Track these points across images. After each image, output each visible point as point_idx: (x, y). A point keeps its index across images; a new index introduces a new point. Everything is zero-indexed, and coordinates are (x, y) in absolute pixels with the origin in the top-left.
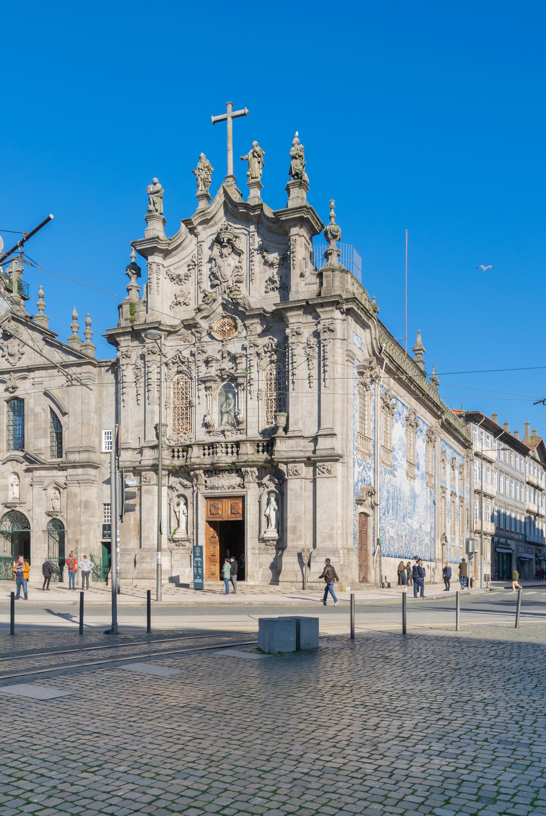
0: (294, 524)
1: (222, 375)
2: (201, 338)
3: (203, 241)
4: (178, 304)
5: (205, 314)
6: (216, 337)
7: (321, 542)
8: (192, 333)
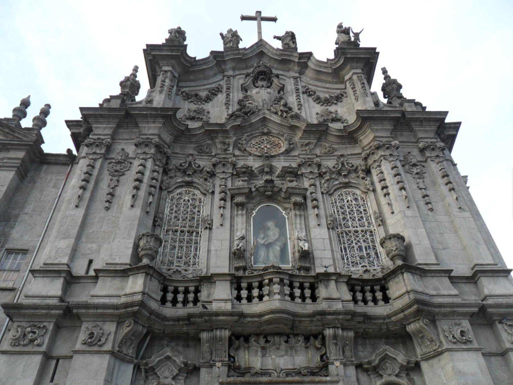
2: (226, 150)
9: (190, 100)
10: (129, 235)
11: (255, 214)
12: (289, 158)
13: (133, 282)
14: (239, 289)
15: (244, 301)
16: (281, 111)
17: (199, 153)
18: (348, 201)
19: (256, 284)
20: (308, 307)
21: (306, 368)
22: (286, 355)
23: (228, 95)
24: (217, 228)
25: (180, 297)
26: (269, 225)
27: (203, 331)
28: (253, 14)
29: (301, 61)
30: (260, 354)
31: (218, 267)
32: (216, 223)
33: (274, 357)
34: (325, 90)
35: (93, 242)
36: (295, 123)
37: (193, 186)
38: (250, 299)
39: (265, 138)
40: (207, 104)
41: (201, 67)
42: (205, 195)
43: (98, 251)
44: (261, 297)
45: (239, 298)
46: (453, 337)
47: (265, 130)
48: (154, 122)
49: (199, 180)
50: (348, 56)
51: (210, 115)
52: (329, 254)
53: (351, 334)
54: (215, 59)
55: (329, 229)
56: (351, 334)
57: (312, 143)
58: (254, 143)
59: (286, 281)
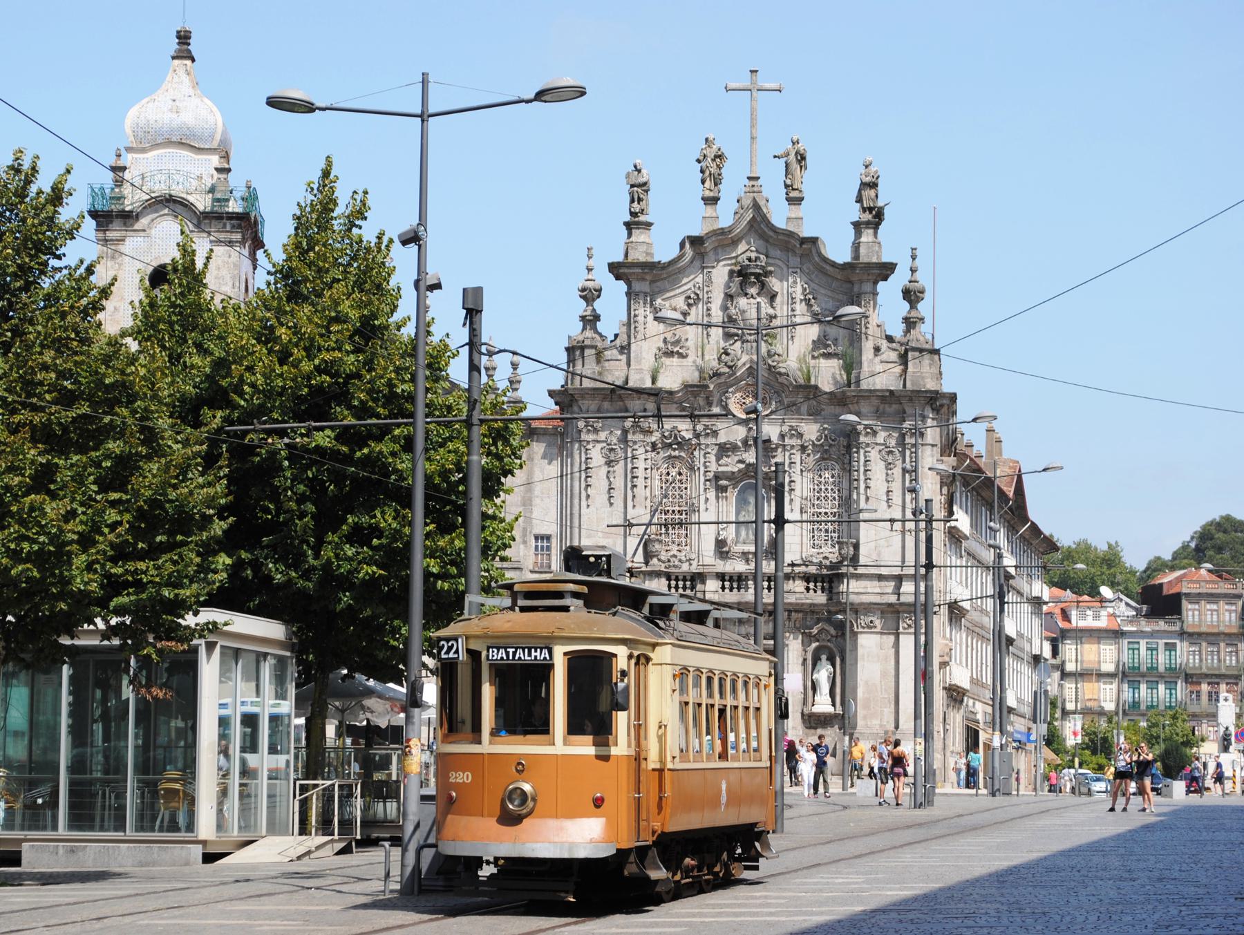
4: (670, 354)
14: (723, 580)
15: (727, 591)
23: (708, 310)
25: (681, 584)
28: (746, 83)
32: (702, 507)
34: (829, 293)
38: (731, 589)
44: (739, 589)
45: (723, 588)
51: (689, 344)
52: (798, 539)
53: (800, 615)
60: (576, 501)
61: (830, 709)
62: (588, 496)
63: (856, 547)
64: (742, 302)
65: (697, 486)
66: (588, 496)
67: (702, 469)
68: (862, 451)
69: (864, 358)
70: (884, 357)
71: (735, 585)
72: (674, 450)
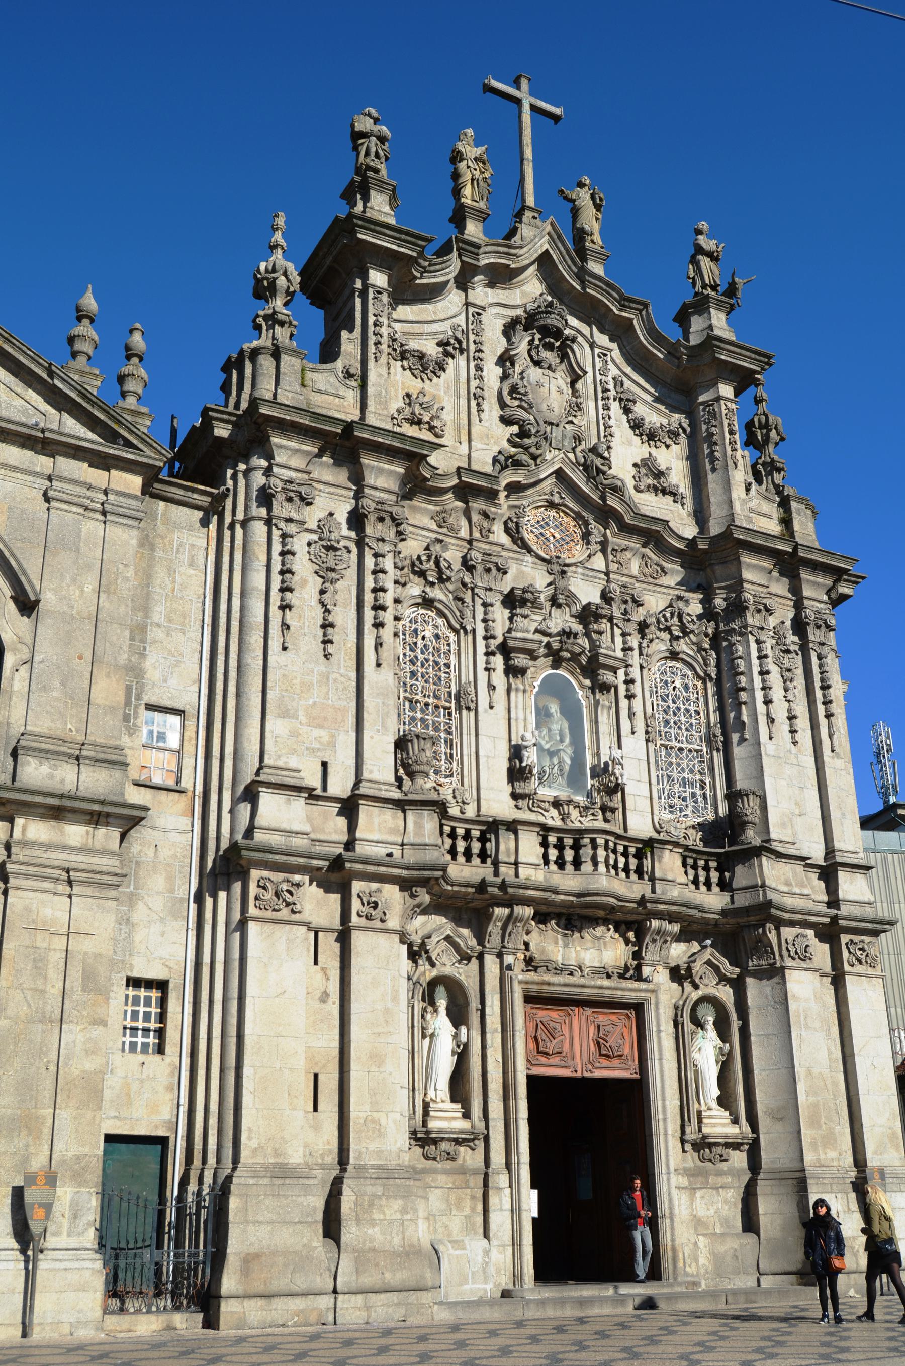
0: (811, 1099)
1: (561, 650)
3: (483, 308)
5: (519, 477)
6: (534, 548)
7: (875, 1153)
8: (467, 514)
9: (405, 363)
10: (384, 725)
11: (537, 689)
12: (592, 574)
13: (415, 823)
14: (545, 844)
16: (597, 468)
17: (440, 526)
18: (674, 689)
19: (568, 841)
20: (635, 886)
21: (615, 967)
22: (593, 948)
24: (486, 711)
26: (553, 710)
27: (499, 905)
29: (624, 314)
30: (560, 942)
31: (492, 789)
33: (578, 948)
35: (320, 726)
36: (612, 501)
37: (436, 608)
39: (552, 513)
40: (435, 379)
41: (435, 277)
42: (456, 632)
43: (332, 744)
44: (577, 863)
46: (796, 953)
47: (556, 499)
48: (390, 462)
49: (446, 595)
50: (723, 357)
54: (460, 256)
55: (647, 741)
56: (676, 928)
57: (632, 549)
58: (532, 522)
59: (611, 845)
60: (255, 639)
61: (734, 1130)
62: (285, 626)
63: (764, 807)
64: (535, 374)
65: (471, 663)
66: (285, 626)
67: (480, 632)
68: (752, 639)
69: (734, 495)
70: (753, 504)
71: (569, 855)
72: (432, 584)
